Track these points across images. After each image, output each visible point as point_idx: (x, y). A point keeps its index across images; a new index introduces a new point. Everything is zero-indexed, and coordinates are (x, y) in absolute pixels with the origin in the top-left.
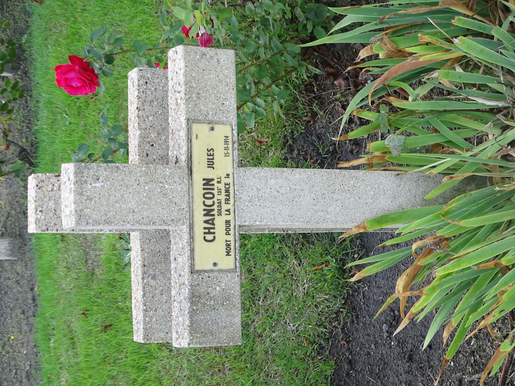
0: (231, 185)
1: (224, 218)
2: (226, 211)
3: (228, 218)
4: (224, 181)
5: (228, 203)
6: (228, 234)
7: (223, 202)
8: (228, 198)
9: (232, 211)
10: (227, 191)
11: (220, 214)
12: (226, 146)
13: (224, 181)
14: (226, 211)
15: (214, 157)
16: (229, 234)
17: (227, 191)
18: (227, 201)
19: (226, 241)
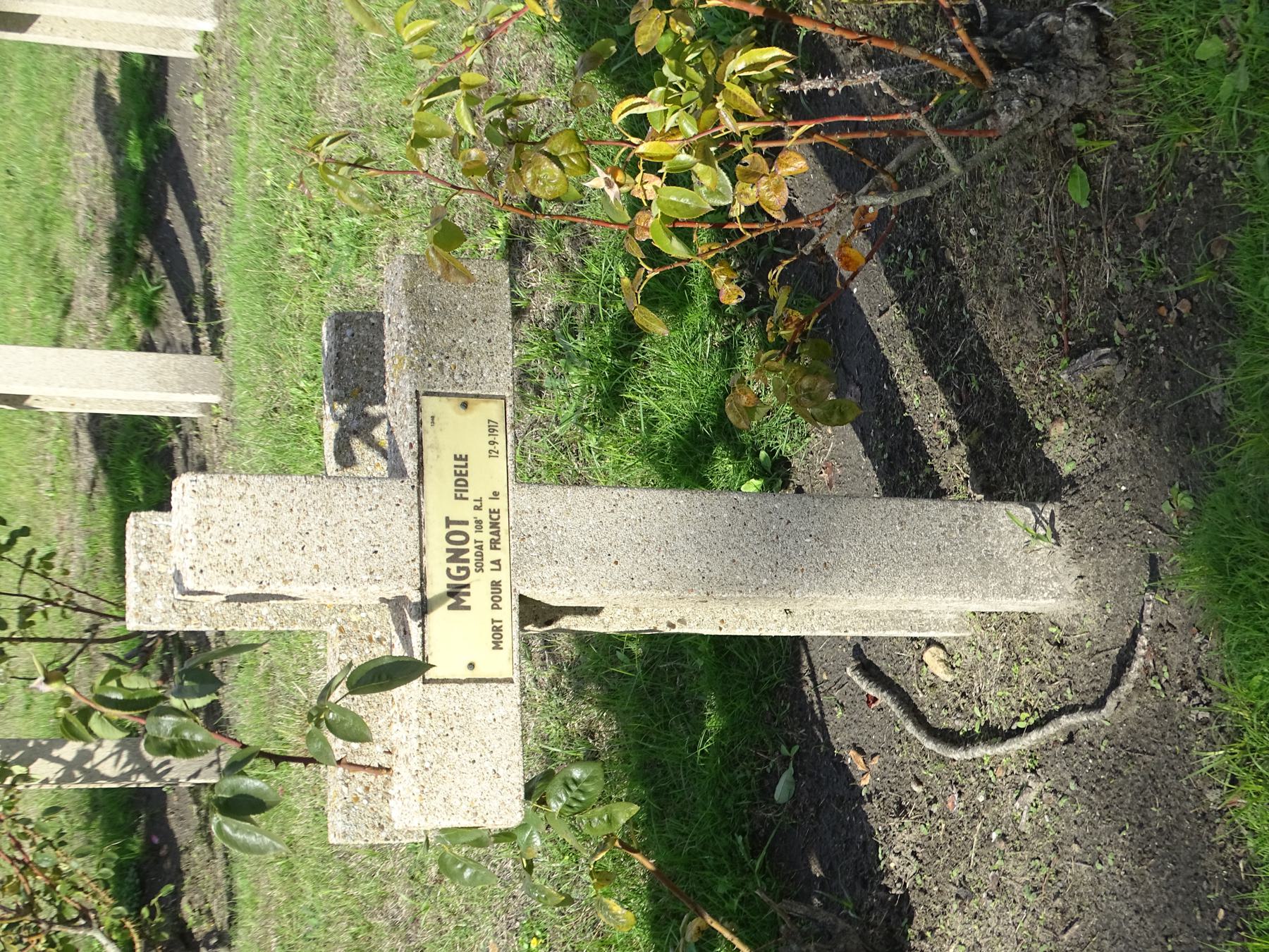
0: (504, 515)
1: (489, 575)
2: (493, 562)
3: (496, 576)
4: (488, 504)
5: (495, 548)
6: (496, 606)
7: (486, 545)
9: (505, 564)
10: (495, 525)
11: (480, 569)
12: (492, 438)
13: (488, 504)
14: (493, 562)
16: (499, 608)
17: (495, 525)
18: (494, 545)
19: (493, 621)
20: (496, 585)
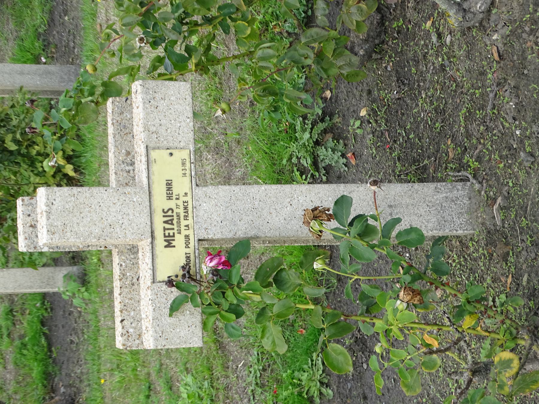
0: (189, 203)
1: (184, 232)
2: (186, 226)
3: (187, 233)
4: (183, 199)
5: (186, 219)
6: (187, 247)
7: (182, 218)
8: (187, 214)
10: (186, 208)
12: (183, 168)
13: (183, 199)
14: (186, 226)
15: (173, 181)
16: (189, 247)
17: (186, 208)
19: (186, 254)
20: (187, 237)
